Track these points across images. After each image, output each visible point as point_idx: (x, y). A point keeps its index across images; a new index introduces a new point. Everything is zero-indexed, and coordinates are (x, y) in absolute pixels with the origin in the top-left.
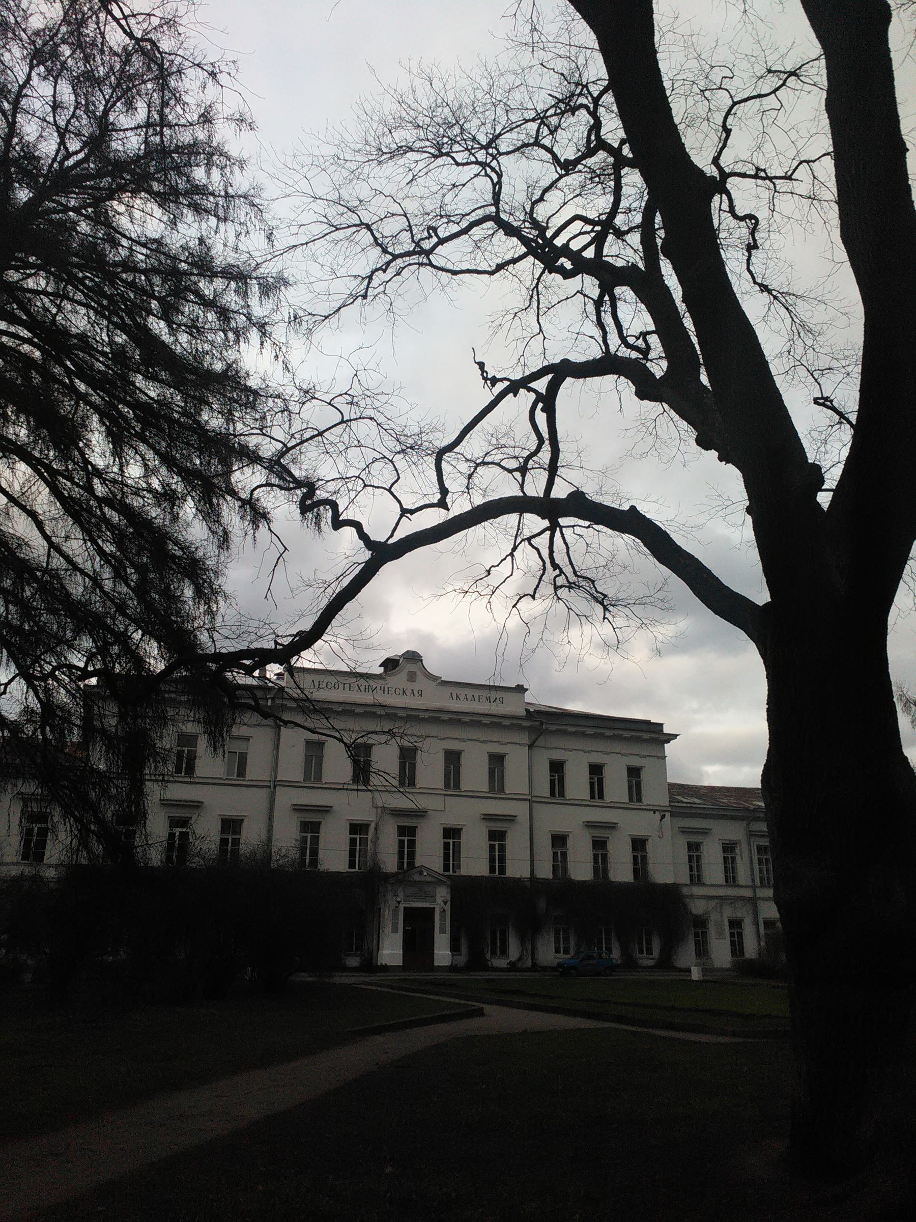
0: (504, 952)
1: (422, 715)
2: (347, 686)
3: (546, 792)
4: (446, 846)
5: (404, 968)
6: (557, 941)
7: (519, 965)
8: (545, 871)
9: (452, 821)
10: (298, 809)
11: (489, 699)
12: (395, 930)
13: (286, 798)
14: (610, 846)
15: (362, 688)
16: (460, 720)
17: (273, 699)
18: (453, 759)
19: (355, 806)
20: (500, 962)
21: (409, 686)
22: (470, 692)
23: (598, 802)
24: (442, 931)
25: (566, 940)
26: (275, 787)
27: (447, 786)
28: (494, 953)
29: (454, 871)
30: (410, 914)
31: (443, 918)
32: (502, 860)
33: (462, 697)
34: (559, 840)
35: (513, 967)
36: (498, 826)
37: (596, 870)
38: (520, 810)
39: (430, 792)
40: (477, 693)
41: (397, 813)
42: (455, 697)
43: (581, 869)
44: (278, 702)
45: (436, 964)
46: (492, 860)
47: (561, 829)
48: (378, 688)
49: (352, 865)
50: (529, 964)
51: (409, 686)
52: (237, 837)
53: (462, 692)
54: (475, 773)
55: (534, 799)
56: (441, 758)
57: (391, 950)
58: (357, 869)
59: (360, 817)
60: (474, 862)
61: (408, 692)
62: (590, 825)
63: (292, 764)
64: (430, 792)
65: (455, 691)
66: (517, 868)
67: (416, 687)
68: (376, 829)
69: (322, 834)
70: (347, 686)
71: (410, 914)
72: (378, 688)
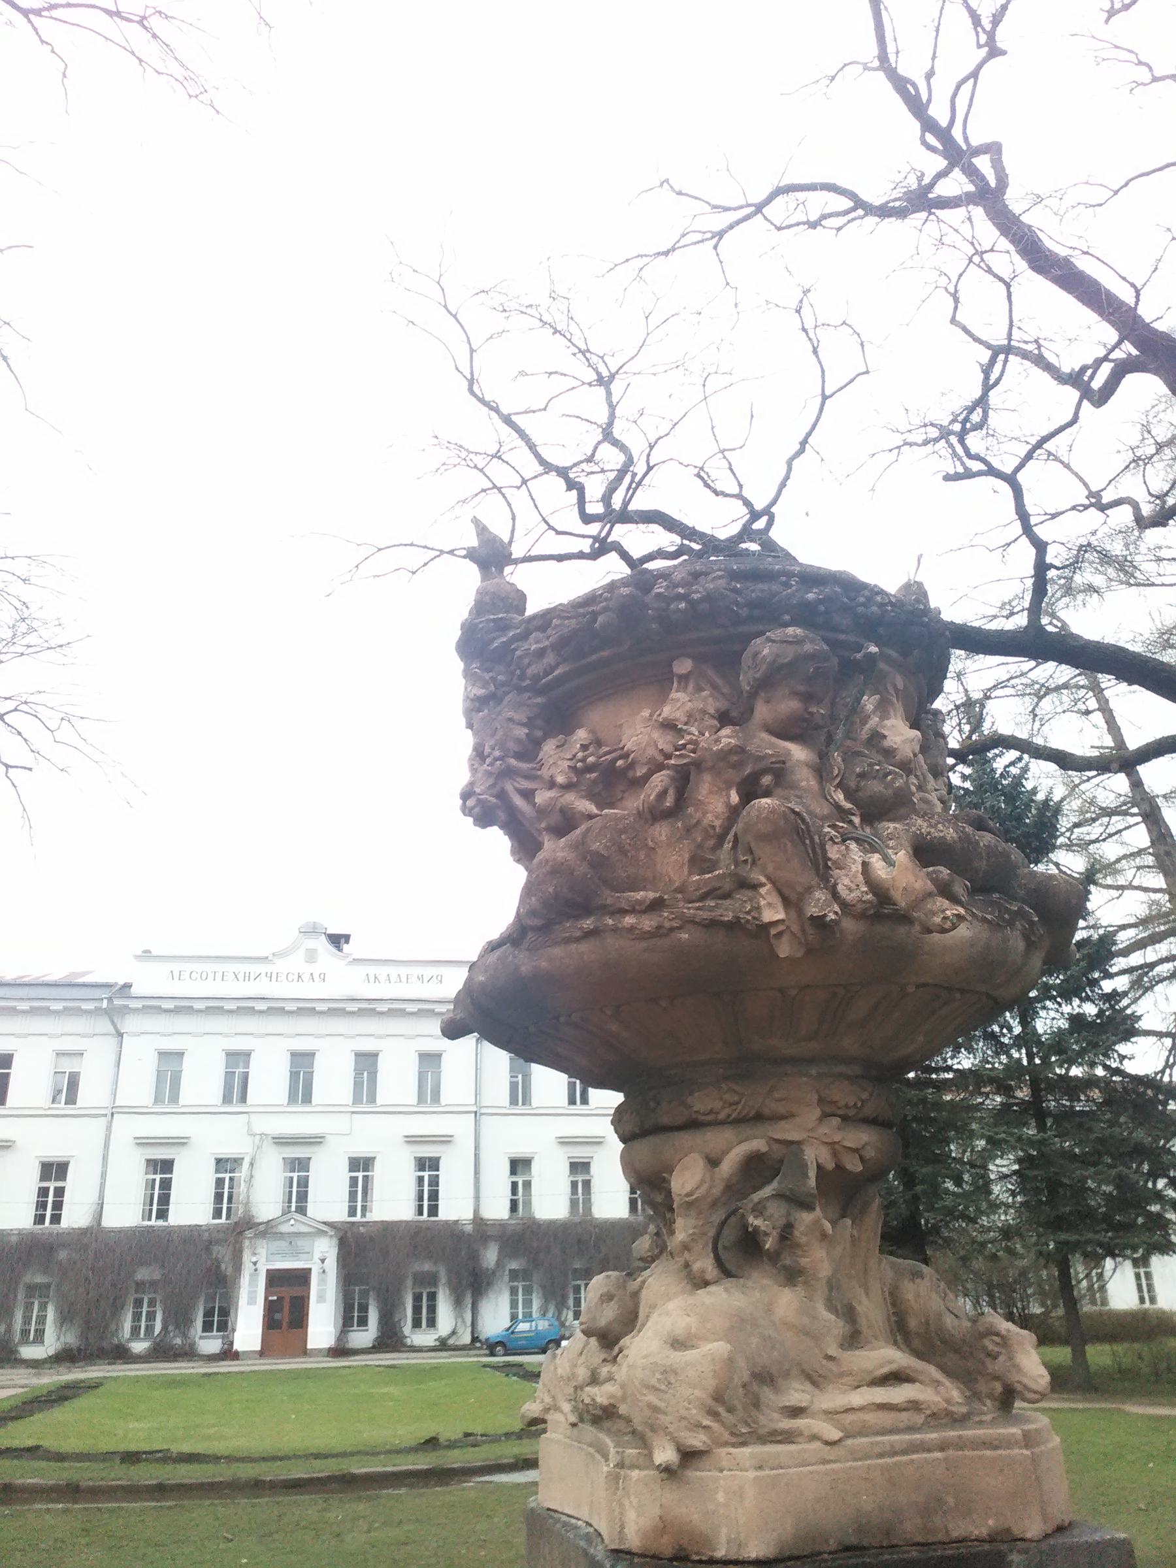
0: (432, 1323)
1: (198, 1005)
2: (219, 976)
3: (504, 1097)
4: (354, 1182)
5: (262, 1354)
6: (514, 1304)
7: (451, 1342)
8: (497, 1209)
9: (361, 1150)
10: (143, 1143)
11: (420, 978)
12: (252, 1301)
13: (127, 1129)
14: (594, 1169)
15: (241, 977)
16: (374, 1010)
17: (110, 999)
18: (367, 1062)
19: (226, 1135)
20: (424, 1338)
21: (306, 969)
22: (393, 971)
23: (579, 1108)
24: (252, 1301)
25: (528, 1303)
26: (112, 1114)
27: (357, 1100)
28: (417, 1324)
29: (363, 1215)
30: (275, 1279)
31: (323, 1281)
32: (434, 1196)
33: (382, 978)
34: (519, 1165)
35: (443, 1345)
36: (580, 1153)
37: (574, 1203)
38: (461, 1128)
39: (331, 1110)
40: (404, 971)
41: (282, 1141)
42: (372, 979)
43: (551, 1203)
44: (117, 1002)
45: (309, 1347)
46: (219, 1197)
47: (520, 1150)
48: (263, 975)
49: (217, 1213)
50: (467, 1339)
51: (306, 969)
52: (60, 1184)
53: (382, 971)
54: (397, 1079)
55: (484, 1111)
56: (349, 1063)
57: (248, 1330)
58: (223, 1220)
59: (228, 1150)
60: (393, 1202)
61: (306, 977)
62: (564, 1142)
63: (139, 1085)
64: (331, 1110)
65: (372, 970)
66: (455, 1207)
67: (316, 969)
68: (252, 1164)
69: (442, 1173)
70: (219, 976)
71: (275, 1279)
72: (263, 975)
